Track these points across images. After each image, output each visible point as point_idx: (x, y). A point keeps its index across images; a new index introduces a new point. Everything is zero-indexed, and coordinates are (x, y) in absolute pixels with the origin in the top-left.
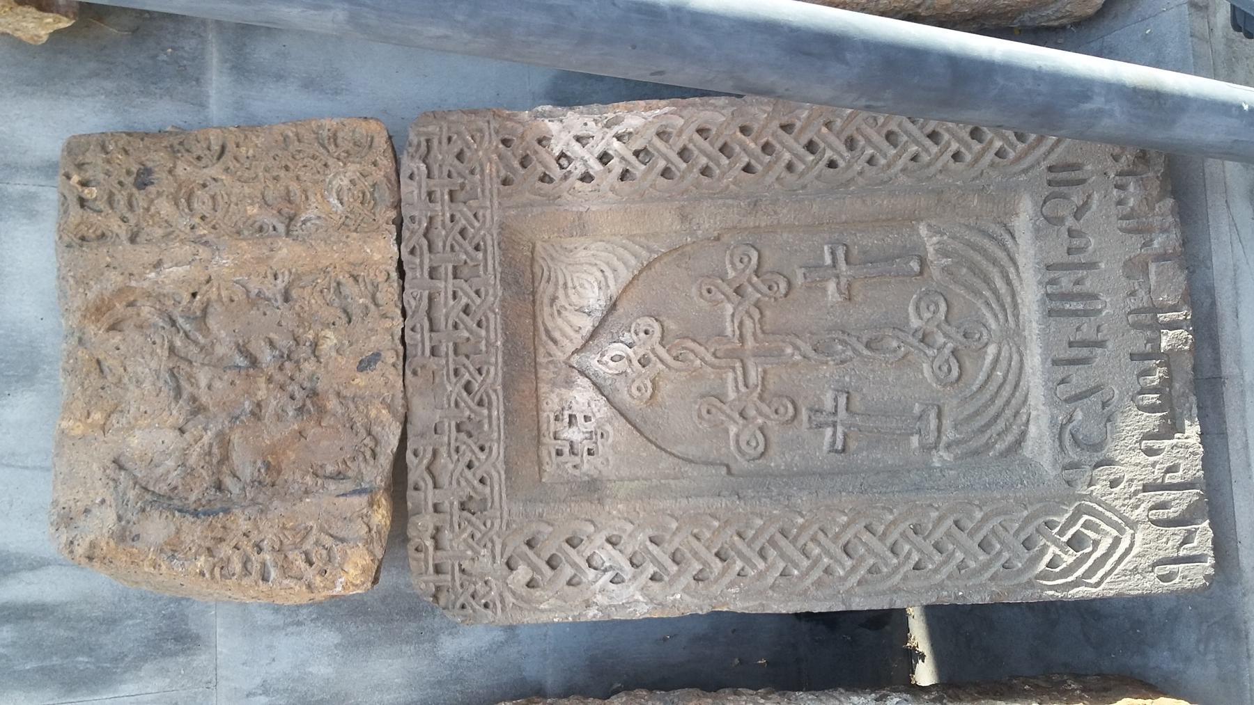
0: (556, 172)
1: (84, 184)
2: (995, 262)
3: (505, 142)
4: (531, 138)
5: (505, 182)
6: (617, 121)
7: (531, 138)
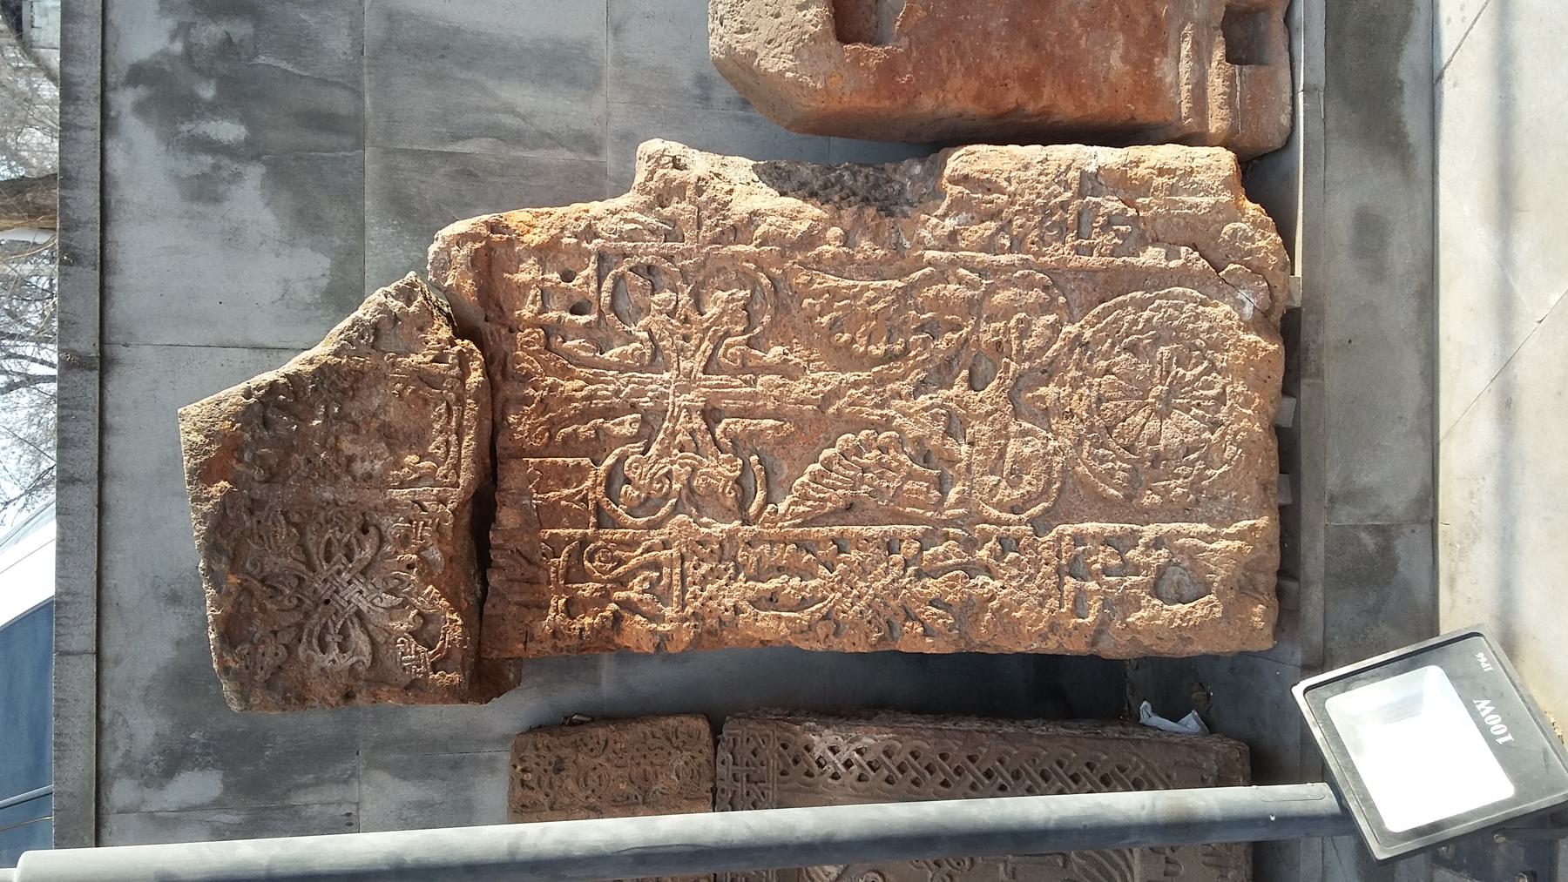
1: (524, 771)
2: (1117, 866)
3: (784, 746)
5: (783, 773)
6: (857, 739)
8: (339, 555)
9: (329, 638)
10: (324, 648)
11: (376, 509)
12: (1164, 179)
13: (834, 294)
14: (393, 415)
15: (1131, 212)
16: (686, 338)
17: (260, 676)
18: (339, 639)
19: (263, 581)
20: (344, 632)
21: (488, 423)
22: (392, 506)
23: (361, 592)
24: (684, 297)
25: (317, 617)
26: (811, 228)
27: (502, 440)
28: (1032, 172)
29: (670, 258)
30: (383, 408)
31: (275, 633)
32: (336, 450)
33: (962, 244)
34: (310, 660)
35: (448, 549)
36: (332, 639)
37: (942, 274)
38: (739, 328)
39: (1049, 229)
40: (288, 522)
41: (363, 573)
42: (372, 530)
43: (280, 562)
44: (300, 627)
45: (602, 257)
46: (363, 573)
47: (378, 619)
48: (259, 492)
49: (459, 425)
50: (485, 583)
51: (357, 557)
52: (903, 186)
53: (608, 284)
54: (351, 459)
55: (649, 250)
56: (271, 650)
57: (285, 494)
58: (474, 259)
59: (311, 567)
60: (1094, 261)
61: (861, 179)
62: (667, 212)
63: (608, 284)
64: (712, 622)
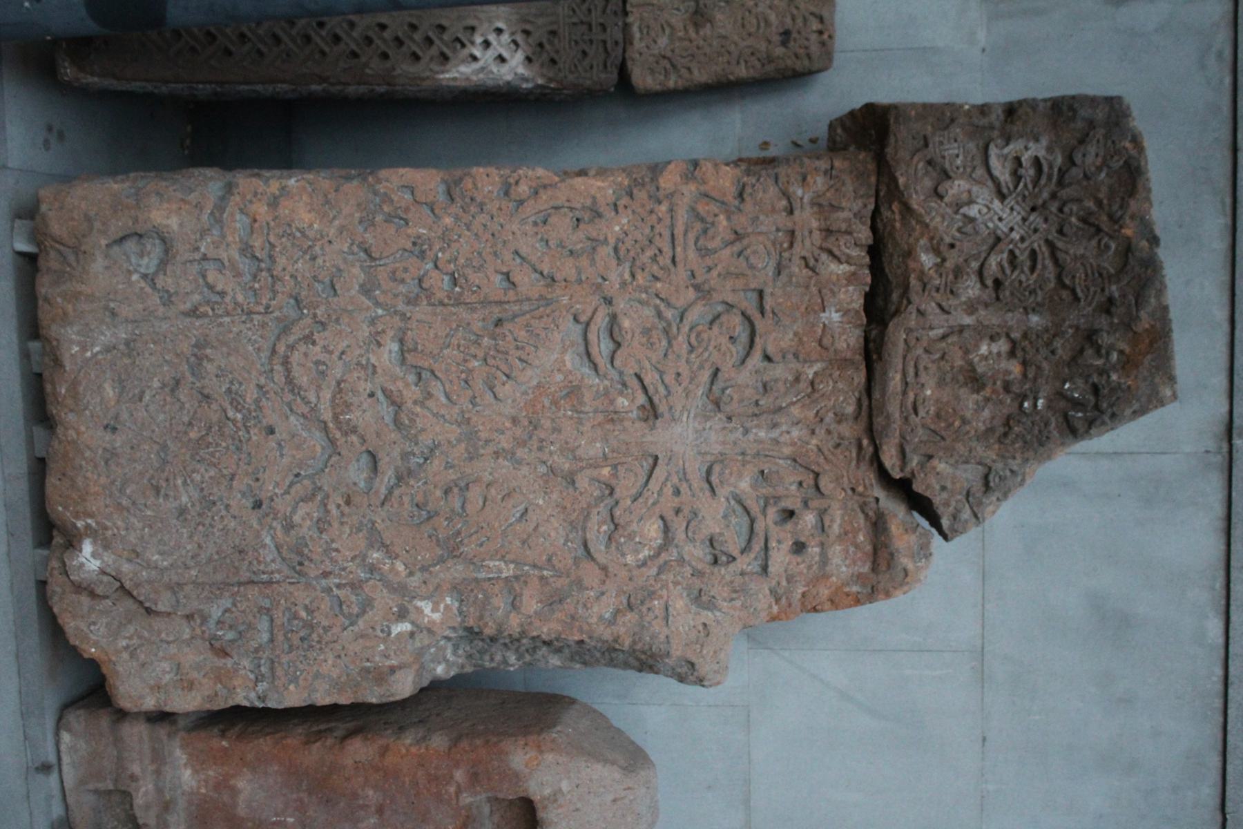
0: (519, 38)
3: (553, 61)
4: (536, 66)
5: (553, 33)
7: (536, 66)
8: (1023, 257)
9: (1032, 172)
10: (1037, 162)
11: (986, 305)
14: (970, 400)
17: (1100, 132)
18: (1022, 171)
19: (1099, 230)
20: (1017, 177)
21: (876, 395)
22: (971, 308)
23: (1000, 219)
25: (1045, 191)
27: (860, 377)
30: (979, 409)
31: (1086, 177)
32: (1025, 363)
34: (1050, 149)
35: (912, 265)
36: (1029, 172)
40: (1073, 291)
41: (998, 240)
42: (989, 282)
43: (1078, 249)
44: (1061, 183)
46: (998, 240)
47: (984, 194)
48: (1103, 322)
49: (904, 393)
50: (874, 228)
51: (1005, 255)
52: (455, 653)
54: (1012, 354)
56: (1090, 159)
57: (1076, 317)
59: (1049, 243)
61: (498, 658)
64: (641, 195)
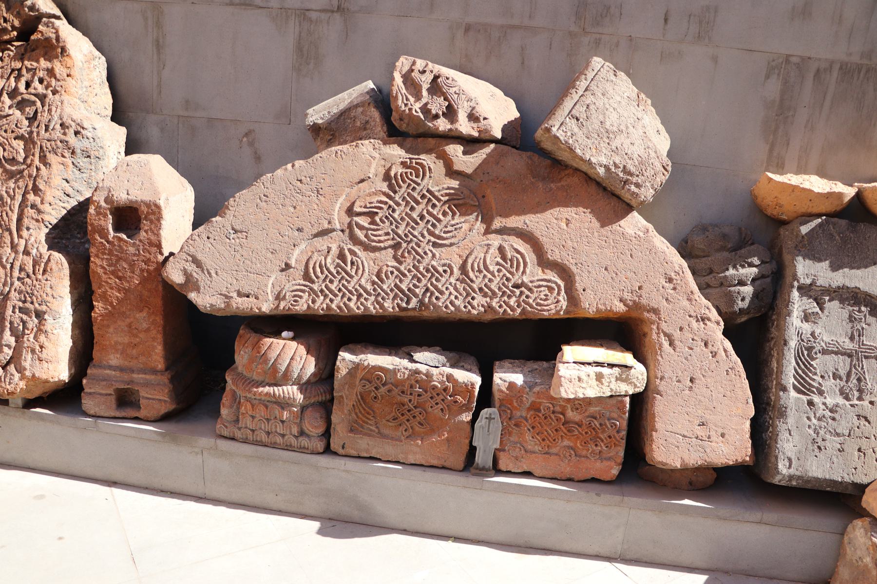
12: (38, 347)
13: (13, 198)
15: (27, 332)
16: (6, 131)
24: (22, 131)
26: (41, 190)
28: (49, 290)
29: (38, 127)
33: (25, 257)
37: (14, 247)
38: (6, 154)
39: (25, 296)
45: (45, 96)
53: (33, 98)
55: (43, 118)
58: (48, 40)
60: (9, 312)
62: (58, 127)
63: (33, 98)
